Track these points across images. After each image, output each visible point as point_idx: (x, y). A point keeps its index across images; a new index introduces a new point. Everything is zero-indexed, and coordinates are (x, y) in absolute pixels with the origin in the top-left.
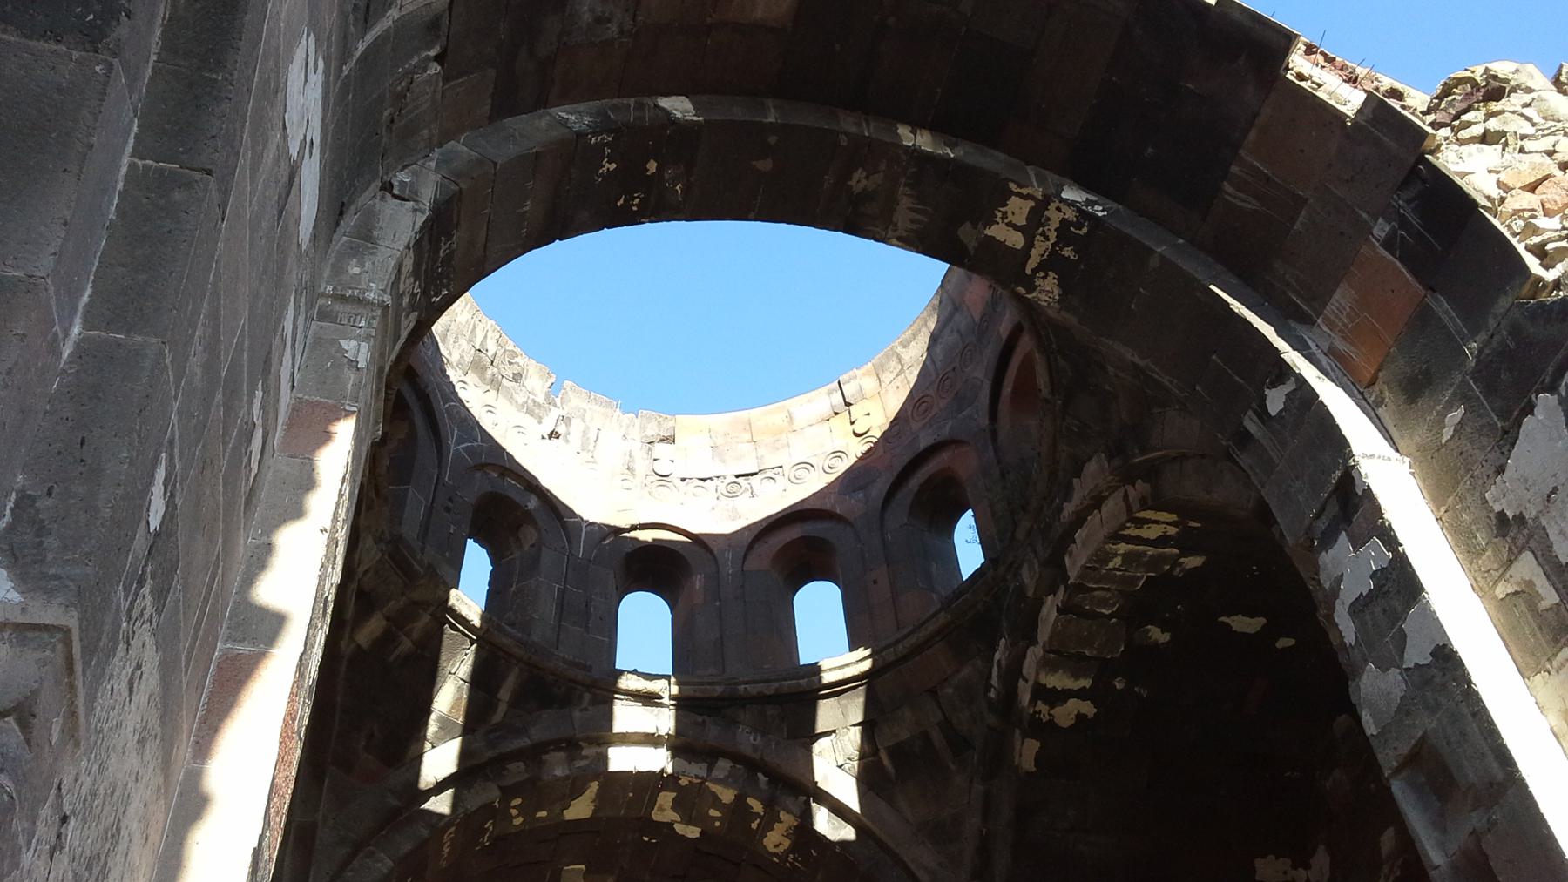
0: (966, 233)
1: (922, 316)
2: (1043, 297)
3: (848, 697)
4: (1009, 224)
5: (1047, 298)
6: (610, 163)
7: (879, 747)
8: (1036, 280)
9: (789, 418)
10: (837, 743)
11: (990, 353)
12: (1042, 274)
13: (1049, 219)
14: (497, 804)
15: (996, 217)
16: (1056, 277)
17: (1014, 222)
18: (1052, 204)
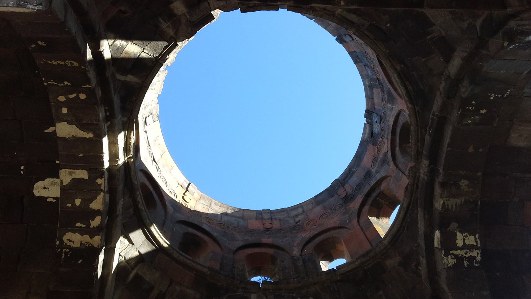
0: (454, 226)
1: (228, 206)
2: (446, 261)
3: (149, 243)
4: (464, 239)
5: (446, 263)
6: (494, 97)
7: (136, 269)
8: (450, 256)
9: (172, 168)
10: (129, 248)
11: (252, 239)
12: (453, 257)
13: (473, 252)
14: (87, 86)
15: (464, 234)
16: (455, 262)
17: (465, 240)
18: (478, 251)
